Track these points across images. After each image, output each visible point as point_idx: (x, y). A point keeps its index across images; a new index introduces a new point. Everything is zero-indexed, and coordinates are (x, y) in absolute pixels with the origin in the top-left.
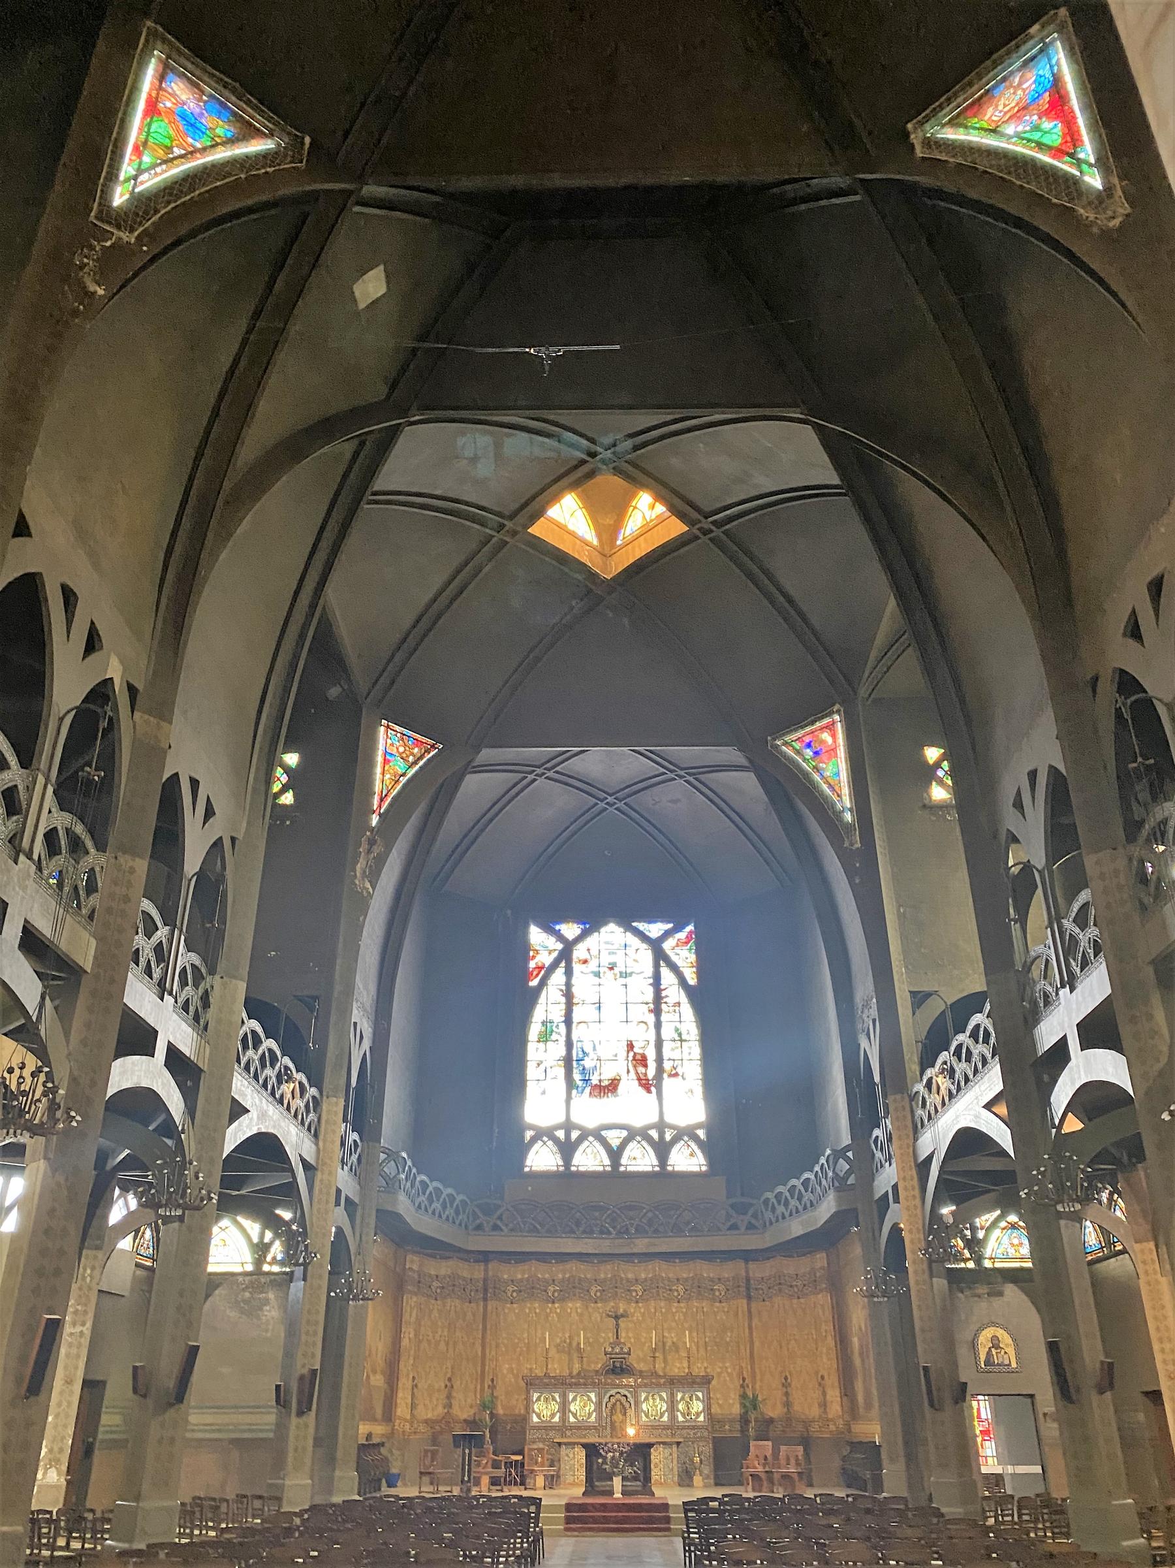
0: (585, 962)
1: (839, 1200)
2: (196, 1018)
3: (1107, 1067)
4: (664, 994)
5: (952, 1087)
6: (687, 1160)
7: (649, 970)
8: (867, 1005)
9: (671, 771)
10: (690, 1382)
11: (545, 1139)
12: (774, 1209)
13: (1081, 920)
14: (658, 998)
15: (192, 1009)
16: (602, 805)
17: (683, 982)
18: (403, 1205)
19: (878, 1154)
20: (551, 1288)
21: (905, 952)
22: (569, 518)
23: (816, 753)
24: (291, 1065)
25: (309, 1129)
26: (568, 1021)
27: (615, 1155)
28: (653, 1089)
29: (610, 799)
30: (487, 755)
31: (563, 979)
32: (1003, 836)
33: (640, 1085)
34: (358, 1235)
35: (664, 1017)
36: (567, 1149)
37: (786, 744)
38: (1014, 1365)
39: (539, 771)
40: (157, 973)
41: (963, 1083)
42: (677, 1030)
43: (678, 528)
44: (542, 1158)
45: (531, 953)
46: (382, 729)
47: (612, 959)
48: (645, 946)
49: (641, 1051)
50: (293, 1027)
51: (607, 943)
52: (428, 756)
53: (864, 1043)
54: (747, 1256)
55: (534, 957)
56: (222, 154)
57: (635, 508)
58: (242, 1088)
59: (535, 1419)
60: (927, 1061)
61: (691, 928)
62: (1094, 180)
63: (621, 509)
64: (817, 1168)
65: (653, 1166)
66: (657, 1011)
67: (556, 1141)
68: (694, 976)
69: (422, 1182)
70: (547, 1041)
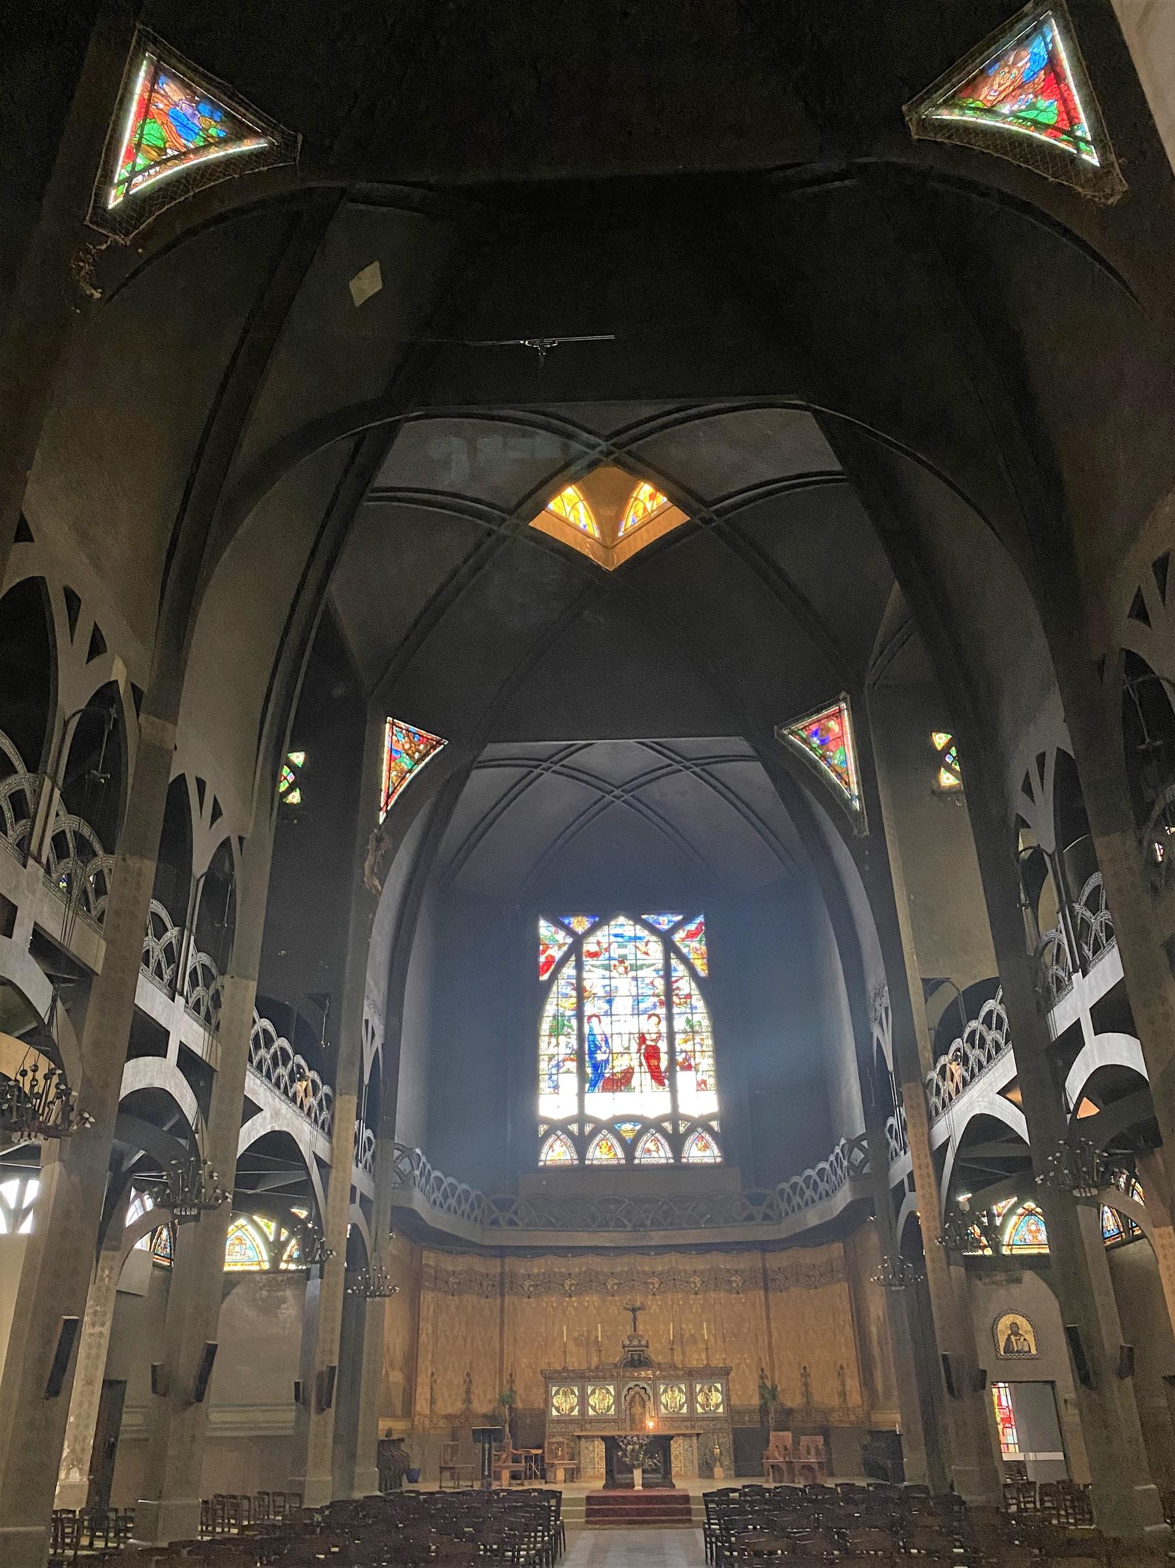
0: (594, 955)
1: (854, 1190)
2: (208, 1018)
3: (1121, 1051)
4: (675, 986)
5: (966, 1074)
6: (701, 1152)
7: (660, 964)
8: (879, 994)
9: (678, 762)
10: (709, 1374)
11: (559, 1133)
12: (789, 1200)
13: (1093, 905)
15: (203, 1009)
16: (609, 798)
18: (419, 1202)
19: (893, 1143)
20: (568, 1282)
21: (917, 939)
22: (570, 511)
23: (823, 742)
24: (303, 1063)
25: (323, 1127)
27: (629, 1148)
28: (666, 1082)
29: (617, 792)
30: (492, 750)
31: (573, 972)
32: (1012, 821)
33: (653, 1077)
34: (373, 1231)
35: (675, 1010)
36: (581, 1143)
37: (793, 733)
38: (1034, 1351)
39: (545, 765)
40: (167, 974)
41: (976, 1070)
42: (688, 1021)
43: (679, 518)
44: (557, 1153)
45: (541, 948)
46: (388, 726)
47: (623, 951)
48: (654, 938)
49: (653, 1044)
50: (305, 1025)
51: (616, 936)
52: (433, 753)
53: (876, 1032)
54: (764, 1247)
55: (544, 951)
56: (215, 154)
57: (636, 499)
58: (255, 1087)
59: (554, 1413)
60: (941, 1049)
61: (701, 919)
62: (1092, 158)
63: (621, 499)
64: (832, 1158)
65: (668, 1159)
67: (570, 1135)
68: (705, 967)
69: (437, 1178)
70: (558, 1035)
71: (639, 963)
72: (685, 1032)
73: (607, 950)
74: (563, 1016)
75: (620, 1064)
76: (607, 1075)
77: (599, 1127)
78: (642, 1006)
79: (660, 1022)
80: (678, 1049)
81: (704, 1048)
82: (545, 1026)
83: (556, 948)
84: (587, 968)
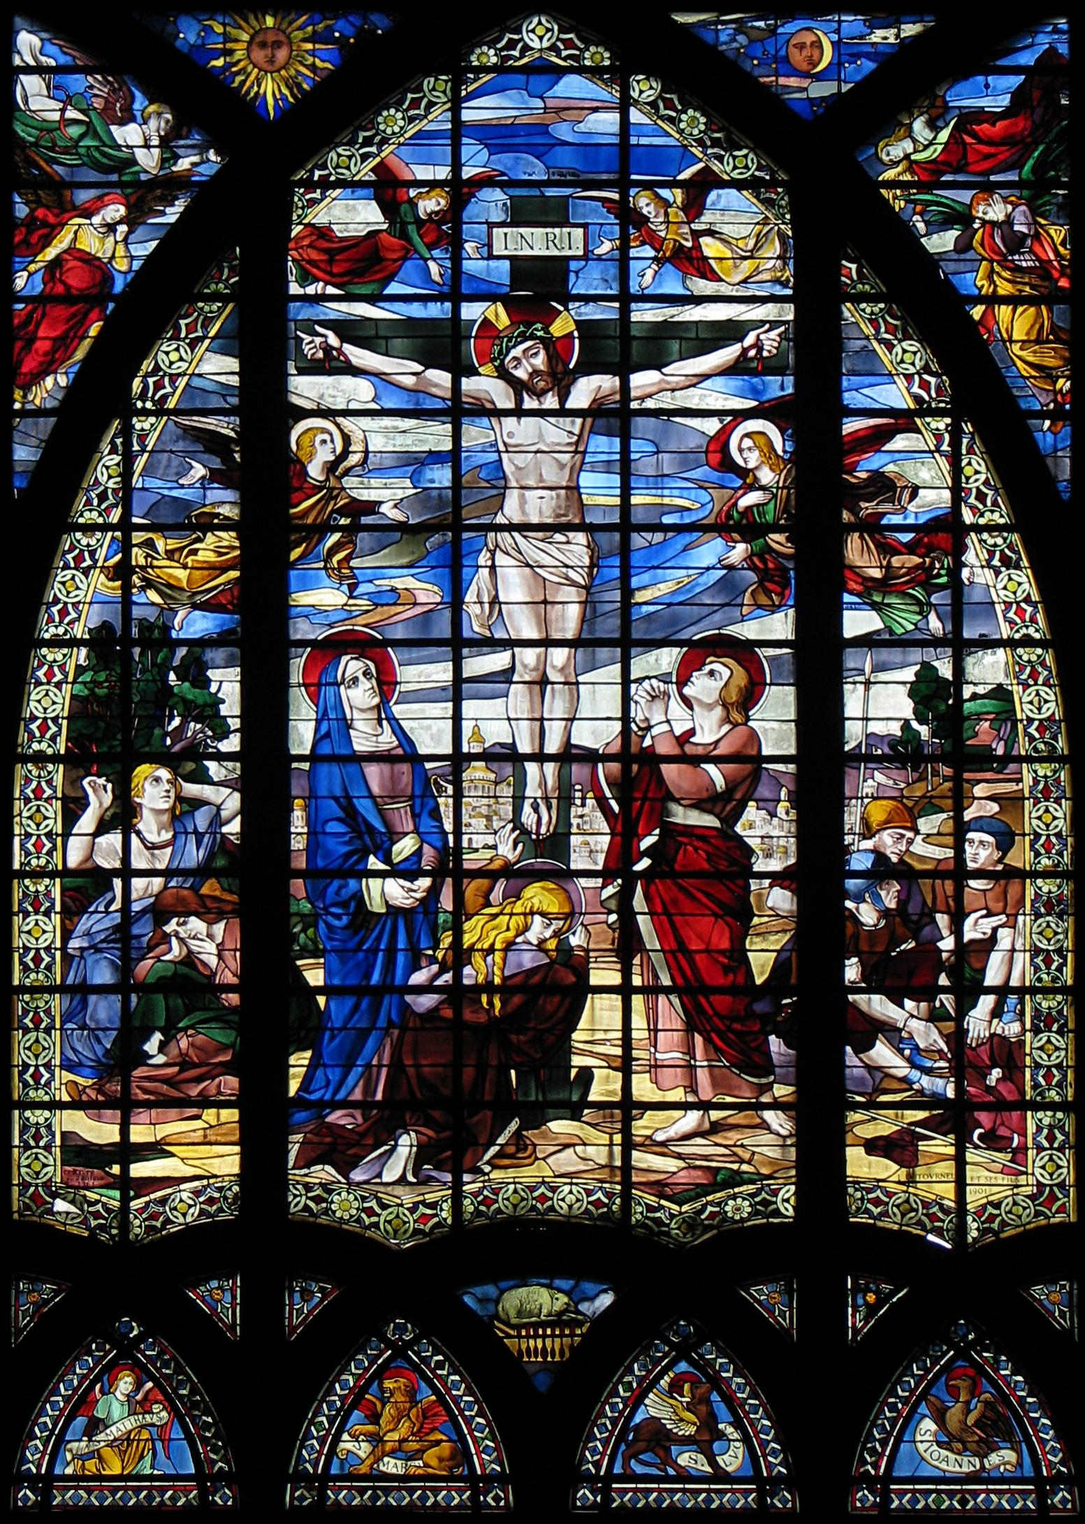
0: (361, 265)
14: (826, 487)
17: (975, 392)
26: (259, 625)
27: (543, 1414)
31: (221, 368)
42: (932, 695)
47: (536, 242)
48: (742, 162)
66: (816, 587)
67: (192, 1335)
71: (644, 314)
72: (902, 752)
73: (448, 232)
74: (158, 637)
75: (507, 936)
76: (426, 1002)
78: (653, 590)
79: (750, 697)
80: (860, 862)
81: (1021, 857)
82: (48, 703)
83: (115, 211)
84: (311, 347)
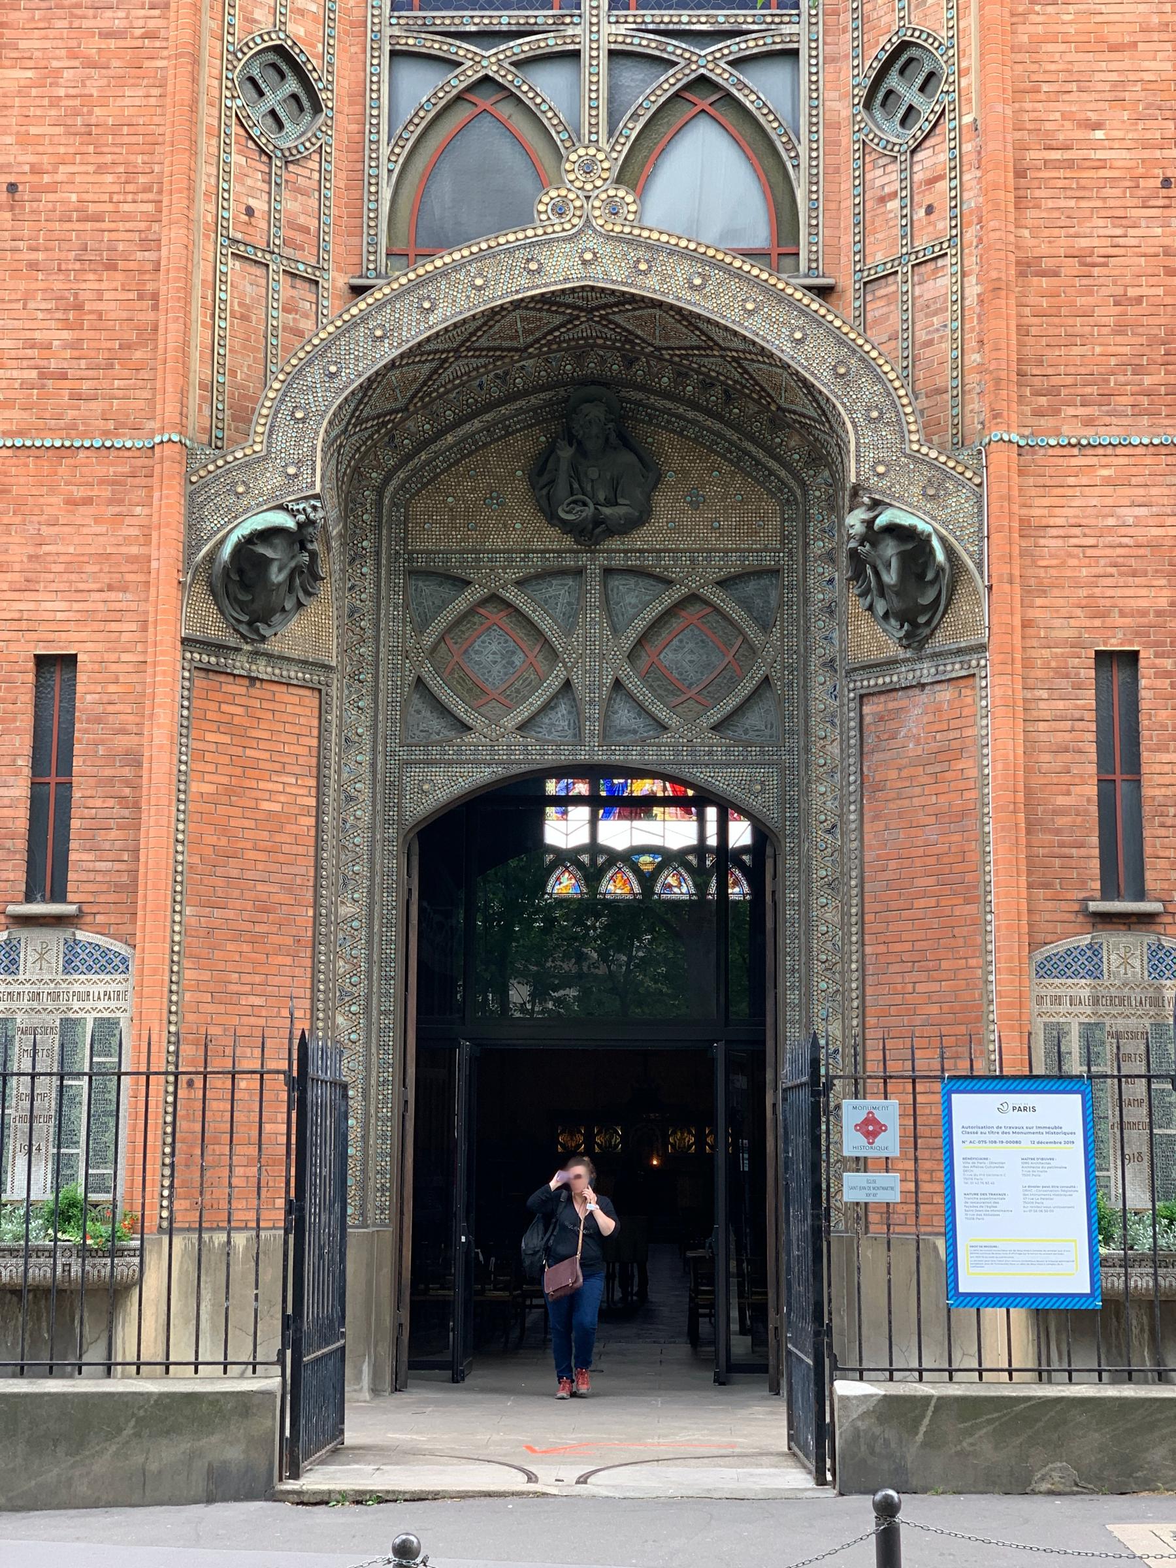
27: (647, 880)
36: (592, 875)
44: (564, 885)
65: (691, 895)
67: (580, 865)
77: (615, 858)
